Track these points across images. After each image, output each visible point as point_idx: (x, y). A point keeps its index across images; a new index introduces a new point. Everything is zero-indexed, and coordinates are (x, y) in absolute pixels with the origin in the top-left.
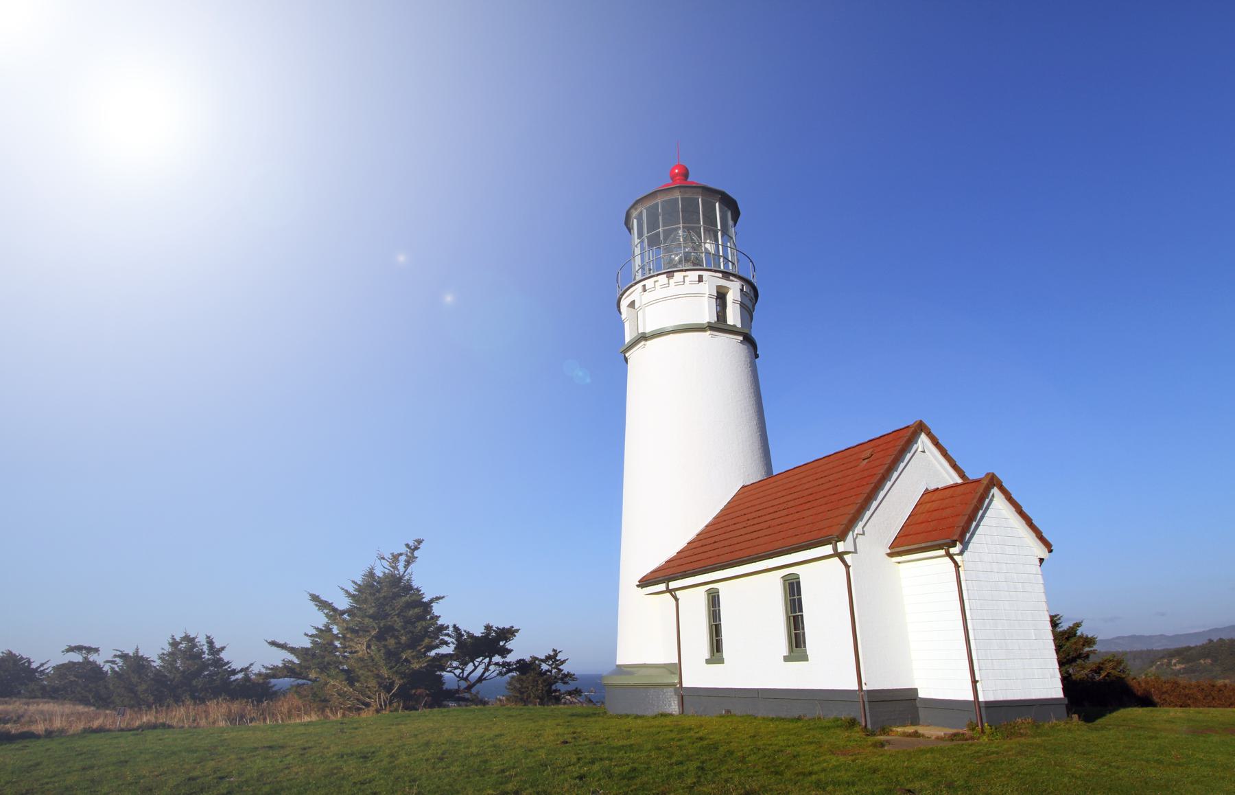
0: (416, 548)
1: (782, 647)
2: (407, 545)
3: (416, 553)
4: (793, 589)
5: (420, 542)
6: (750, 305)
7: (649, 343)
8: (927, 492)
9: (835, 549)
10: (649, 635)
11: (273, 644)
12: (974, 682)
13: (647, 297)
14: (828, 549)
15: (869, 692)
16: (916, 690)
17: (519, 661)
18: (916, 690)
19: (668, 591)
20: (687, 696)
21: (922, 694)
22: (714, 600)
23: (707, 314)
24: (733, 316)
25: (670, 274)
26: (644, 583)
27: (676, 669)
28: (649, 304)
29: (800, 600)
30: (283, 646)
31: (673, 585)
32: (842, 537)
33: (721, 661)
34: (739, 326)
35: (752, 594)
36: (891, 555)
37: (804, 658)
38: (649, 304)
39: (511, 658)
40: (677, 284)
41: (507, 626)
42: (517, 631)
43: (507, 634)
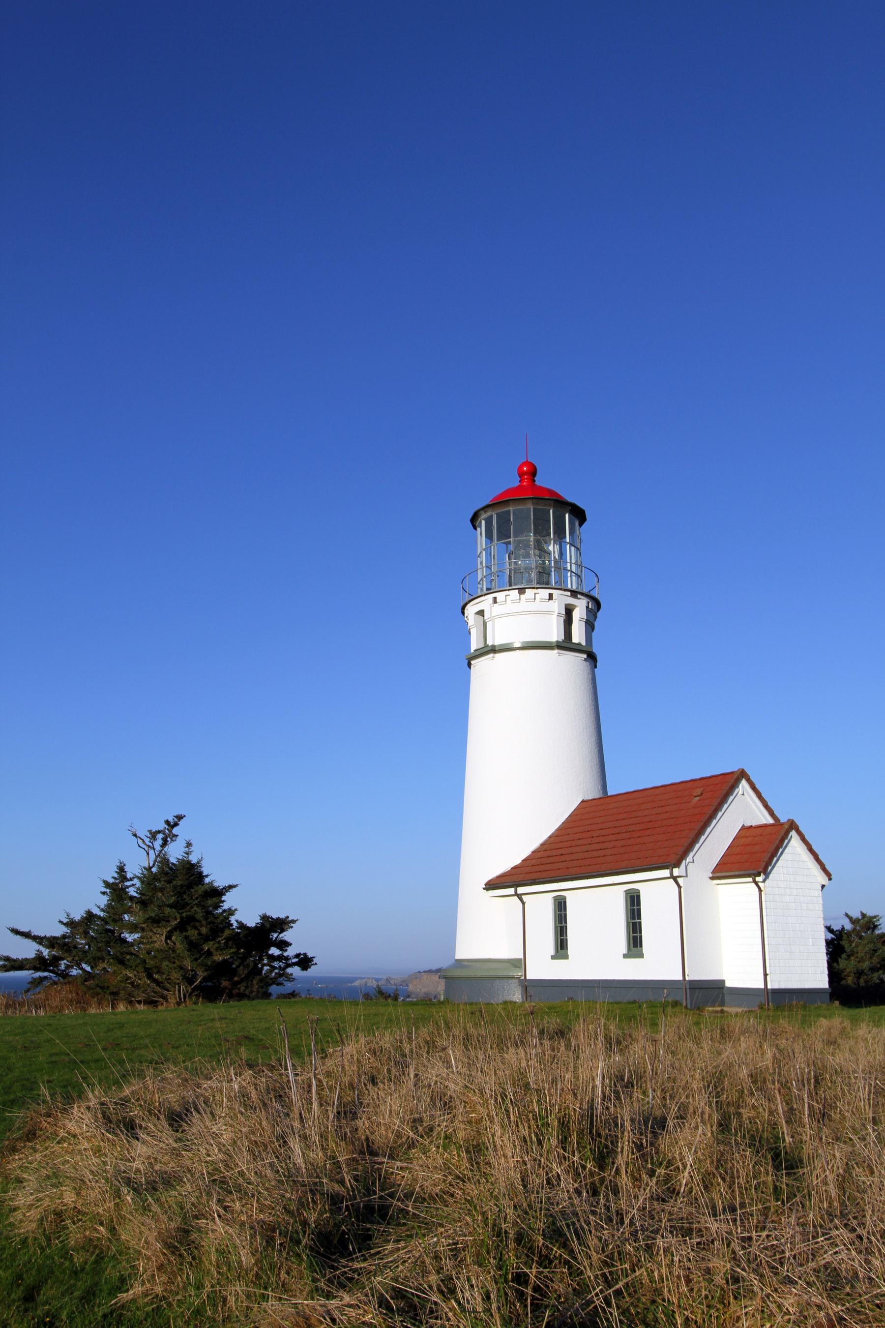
0: (176, 824)
1: (623, 947)
2: (167, 822)
3: (175, 831)
4: (633, 901)
5: (180, 818)
6: (592, 620)
7: (497, 655)
8: (744, 828)
9: (671, 873)
10: (493, 931)
11: (16, 932)
12: (765, 975)
14: (666, 873)
15: (691, 982)
16: (723, 981)
17: (297, 956)
18: (723, 981)
19: (516, 894)
20: (528, 986)
21: (728, 984)
22: (561, 906)
23: (555, 634)
24: (578, 635)
25: (522, 591)
26: (491, 886)
27: (520, 964)
28: (499, 616)
29: (639, 911)
30: (27, 935)
31: (521, 890)
32: (677, 865)
33: (566, 957)
34: (584, 643)
35: (596, 904)
36: (712, 878)
37: (641, 955)
38: (499, 616)
40: (528, 601)
41: (282, 916)
42: (294, 921)
43: (282, 924)
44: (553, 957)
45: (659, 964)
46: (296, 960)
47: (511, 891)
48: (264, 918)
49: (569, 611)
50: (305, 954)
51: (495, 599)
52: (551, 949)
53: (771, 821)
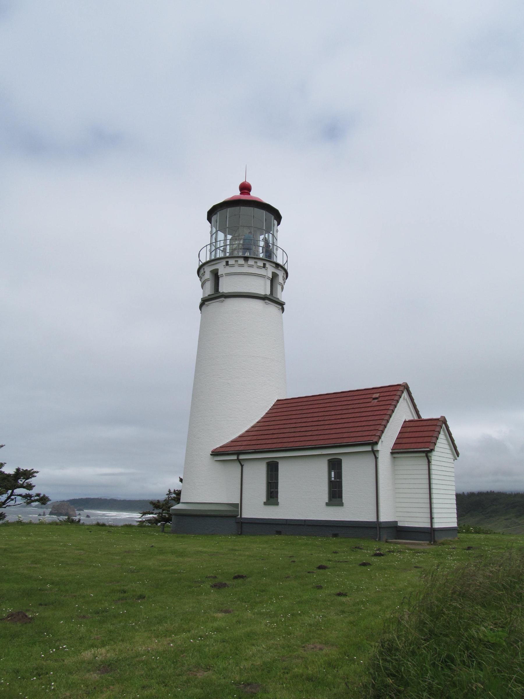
1: (325, 497)
8: (405, 422)
13: (229, 270)
17: (38, 495)
19: (239, 460)
25: (246, 259)
26: (215, 453)
27: (238, 507)
28: (228, 274)
31: (242, 457)
33: (277, 504)
38: (228, 274)
39: (33, 492)
41: (29, 469)
43: (28, 474)
44: (265, 504)
45: (355, 508)
46: (36, 498)
47: (235, 457)
48: (18, 470)
49: (275, 276)
50: (44, 495)
51: (227, 262)
52: (263, 498)
53: (416, 418)
